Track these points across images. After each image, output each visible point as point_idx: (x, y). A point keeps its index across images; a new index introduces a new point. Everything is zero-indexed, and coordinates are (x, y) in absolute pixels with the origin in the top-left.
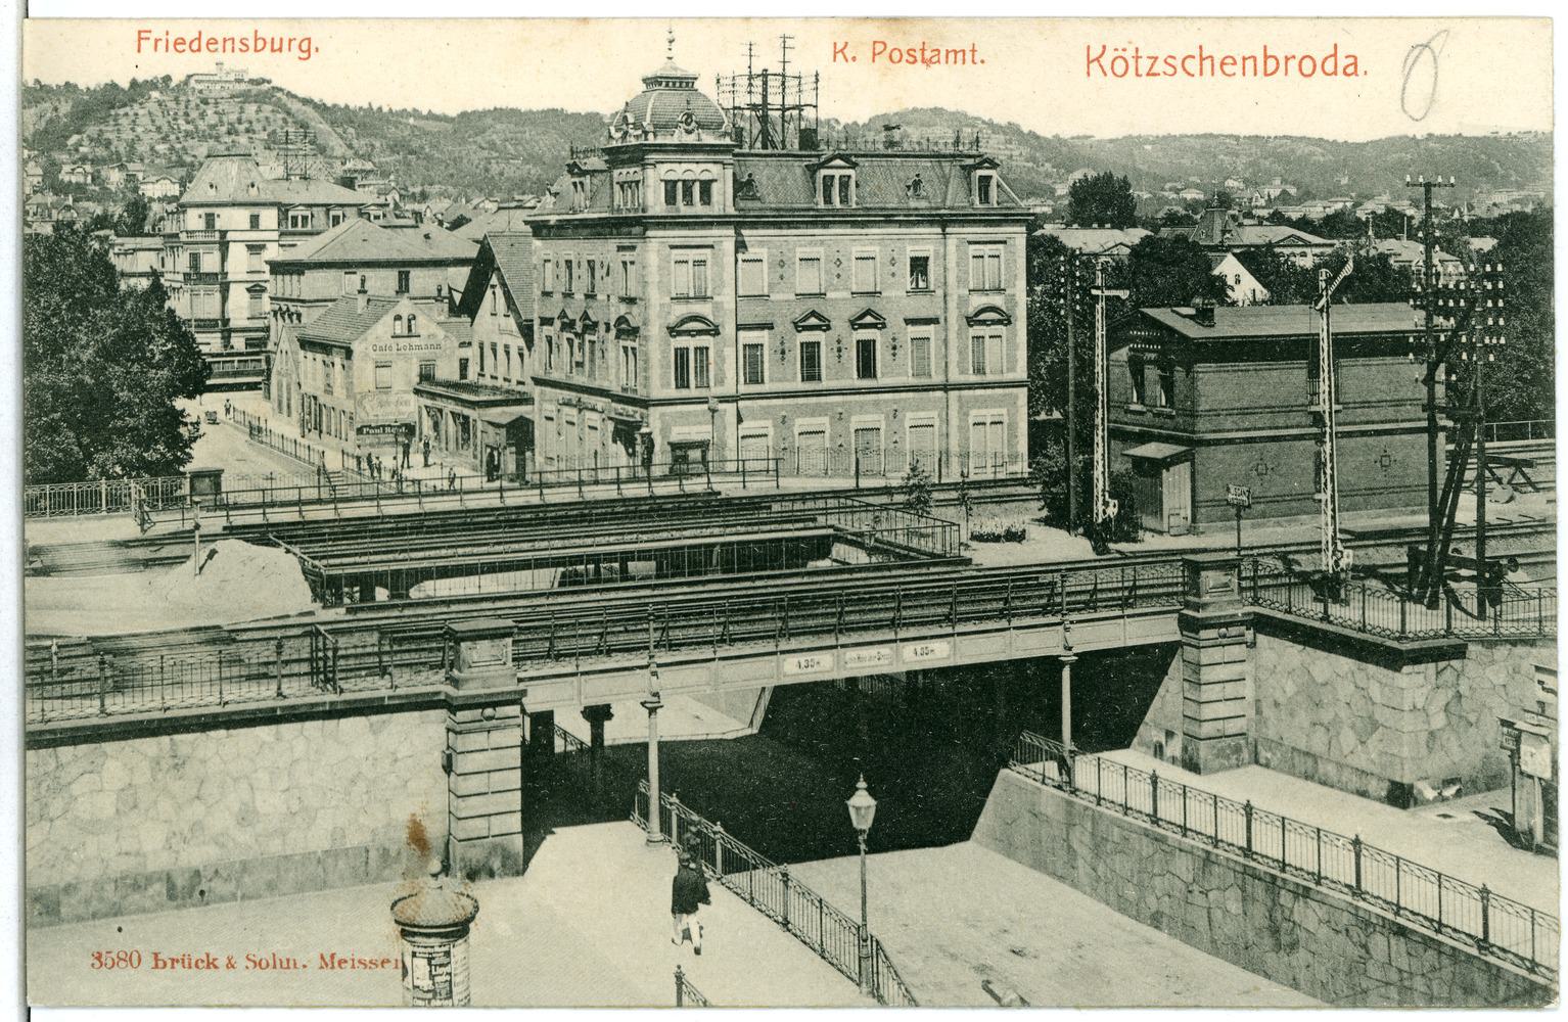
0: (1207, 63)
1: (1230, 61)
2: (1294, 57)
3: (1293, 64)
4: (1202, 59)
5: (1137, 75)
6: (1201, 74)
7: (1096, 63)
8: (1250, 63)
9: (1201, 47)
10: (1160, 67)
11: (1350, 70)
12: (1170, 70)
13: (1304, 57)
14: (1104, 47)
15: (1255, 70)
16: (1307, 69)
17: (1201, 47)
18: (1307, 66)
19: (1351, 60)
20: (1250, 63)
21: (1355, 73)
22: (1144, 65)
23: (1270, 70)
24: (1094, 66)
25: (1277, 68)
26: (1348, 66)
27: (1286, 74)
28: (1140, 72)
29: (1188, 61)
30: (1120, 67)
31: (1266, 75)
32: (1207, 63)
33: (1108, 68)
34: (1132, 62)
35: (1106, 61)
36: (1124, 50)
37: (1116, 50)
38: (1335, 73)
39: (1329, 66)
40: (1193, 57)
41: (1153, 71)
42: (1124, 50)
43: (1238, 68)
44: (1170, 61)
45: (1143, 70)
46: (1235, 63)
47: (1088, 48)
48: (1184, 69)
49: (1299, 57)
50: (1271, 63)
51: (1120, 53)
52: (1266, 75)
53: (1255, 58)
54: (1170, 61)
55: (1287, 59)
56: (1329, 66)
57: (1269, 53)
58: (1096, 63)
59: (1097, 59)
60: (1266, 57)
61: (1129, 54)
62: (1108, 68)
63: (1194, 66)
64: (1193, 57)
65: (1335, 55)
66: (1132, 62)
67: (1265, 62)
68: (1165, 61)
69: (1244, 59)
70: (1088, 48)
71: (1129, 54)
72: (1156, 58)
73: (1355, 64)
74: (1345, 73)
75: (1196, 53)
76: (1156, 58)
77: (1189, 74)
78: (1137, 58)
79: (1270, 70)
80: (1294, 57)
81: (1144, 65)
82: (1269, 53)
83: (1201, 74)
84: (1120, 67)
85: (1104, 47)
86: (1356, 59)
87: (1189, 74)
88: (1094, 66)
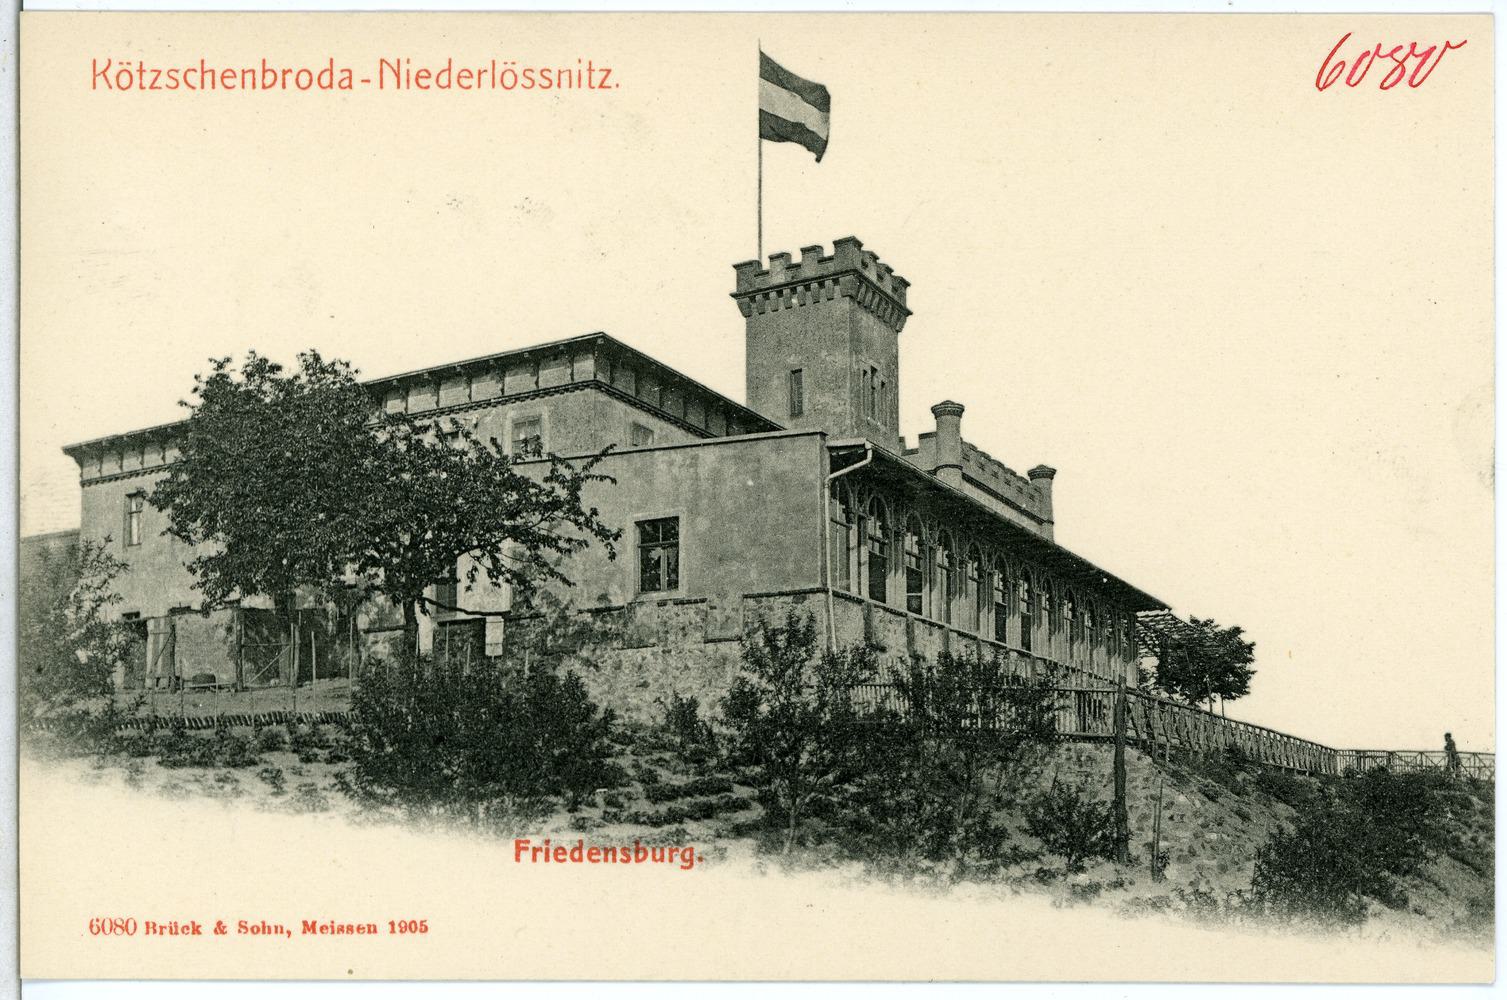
0: (208, 77)
1: (229, 74)
2: (290, 71)
3: (290, 78)
4: (203, 73)
5: (142, 87)
6: (202, 87)
8: (249, 77)
9: (203, 62)
10: (163, 80)
11: (345, 83)
12: (173, 84)
14: (110, 61)
15: (213, 83)
17: (203, 62)
18: (304, 79)
19: (347, 74)
20: (249, 77)
21: (350, 86)
22: (148, 78)
24: (100, 80)
25: (275, 80)
26: (342, 80)
27: (284, 86)
28: (144, 85)
29: (189, 75)
30: (125, 80)
31: (264, 87)
32: (208, 77)
33: (113, 81)
35: (111, 74)
36: (129, 64)
37: (121, 63)
38: (331, 86)
40: (195, 70)
42: (129, 64)
43: (237, 82)
44: (172, 74)
45: (147, 83)
49: (295, 71)
52: (264, 87)
53: (253, 72)
54: (172, 74)
55: (285, 72)
57: (267, 67)
59: (104, 72)
60: (264, 71)
61: (134, 69)
62: (113, 81)
63: (195, 79)
64: (195, 70)
67: (264, 77)
69: (244, 72)
71: (134, 69)
72: (160, 72)
73: (350, 78)
77: (189, 85)
78: (141, 71)
79: (268, 82)
80: (290, 71)
81: (148, 78)
82: (267, 67)
83: (202, 87)
84: (125, 80)
85: (110, 61)
86: (350, 71)
87: (189, 85)
88: (100, 80)
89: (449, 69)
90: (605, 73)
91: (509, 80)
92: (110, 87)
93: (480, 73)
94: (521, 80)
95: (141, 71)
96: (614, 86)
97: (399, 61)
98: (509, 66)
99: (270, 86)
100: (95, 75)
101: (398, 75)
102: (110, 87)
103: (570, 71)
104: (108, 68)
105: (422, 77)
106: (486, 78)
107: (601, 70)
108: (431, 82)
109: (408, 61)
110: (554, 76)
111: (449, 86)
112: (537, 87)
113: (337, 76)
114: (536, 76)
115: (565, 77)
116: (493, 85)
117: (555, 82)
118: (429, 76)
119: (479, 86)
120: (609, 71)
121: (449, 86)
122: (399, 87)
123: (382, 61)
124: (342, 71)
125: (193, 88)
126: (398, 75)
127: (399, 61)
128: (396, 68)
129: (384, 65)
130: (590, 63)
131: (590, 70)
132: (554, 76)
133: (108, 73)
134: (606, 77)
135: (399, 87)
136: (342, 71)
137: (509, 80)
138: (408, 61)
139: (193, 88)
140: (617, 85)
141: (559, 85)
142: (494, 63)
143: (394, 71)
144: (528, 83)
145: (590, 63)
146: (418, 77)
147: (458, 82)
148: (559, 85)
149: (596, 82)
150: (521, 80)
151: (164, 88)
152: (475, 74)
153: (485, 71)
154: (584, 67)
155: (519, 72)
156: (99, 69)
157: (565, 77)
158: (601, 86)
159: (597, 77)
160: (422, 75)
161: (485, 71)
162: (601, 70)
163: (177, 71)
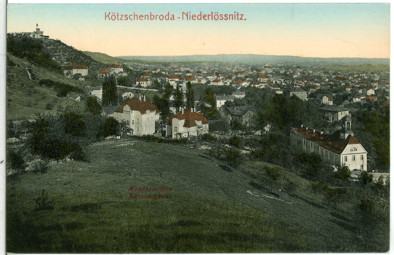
0: (136, 17)
1: (142, 16)
2: (158, 15)
3: (158, 17)
4: (134, 16)
5: (118, 20)
6: (134, 19)
7: (107, 17)
8: (147, 17)
9: (134, 13)
10: (124, 18)
11: (172, 18)
12: (126, 18)
13: (161, 15)
14: (110, 13)
16: (161, 18)
17: (134, 13)
18: (161, 17)
19: (172, 16)
20: (147, 17)
21: (173, 19)
23: (152, 18)
24: (107, 17)
26: (171, 18)
27: (156, 19)
30: (113, 18)
31: (151, 20)
32: (136, 17)
33: (110, 18)
34: (117, 16)
35: (110, 16)
36: (115, 13)
38: (168, 19)
39: (167, 17)
40: (132, 15)
41: (122, 19)
42: (115, 13)
43: (144, 18)
44: (126, 16)
46: (143, 17)
47: (106, 13)
48: (130, 18)
49: (159, 15)
51: (114, 14)
52: (151, 20)
53: (148, 16)
54: (126, 16)
56: (167, 17)
58: (107, 17)
59: (108, 16)
60: (151, 15)
61: (116, 15)
62: (110, 18)
63: (132, 17)
65: (168, 15)
66: (117, 16)
69: (145, 16)
70: (106, 13)
71: (116, 15)
73: (173, 17)
74: (171, 19)
75: (133, 15)
76: (123, 16)
78: (118, 15)
79: (152, 18)
80: (158, 15)
82: (152, 14)
83: (134, 19)
84: (113, 18)
85: (110, 13)
86: (174, 15)
88: (107, 17)
89: (201, 15)
90: (241, 16)
91: (216, 17)
92: (110, 19)
93: (209, 15)
94: (220, 17)
95: (118, 15)
96: (244, 19)
97: (187, 12)
98: (216, 14)
99: (152, 20)
100: (106, 16)
101: (187, 16)
102: (110, 19)
103: (232, 15)
104: (109, 14)
105: (193, 17)
106: (210, 17)
107: (241, 15)
108: (196, 18)
109: (190, 13)
110: (228, 17)
111: (201, 19)
112: (224, 19)
113: (170, 16)
114: (224, 17)
115: (231, 16)
116: (212, 19)
117: (229, 19)
118: (195, 17)
119: (208, 19)
120: (242, 15)
121: (201, 19)
122: (187, 19)
123: (183, 13)
124: (172, 15)
125: (132, 20)
126: (187, 16)
127: (187, 12)
128: (187, 14)
129: (184, 13)
130: (238, 13)
131: (238, 15)
132: (228, 16)
133: (109, 16)
134: (242, 17)
135: (187, 19)
136: (172, 15)
137: (216, 17)
138: (190, 13)
139: (132, 20)
140: (245, 20)
141: (230, 19)
142: (212, 13)
143: (186, 15)
144: (221, 18)
145: (238, 13)
146: (192, 17)
147: (204, 17)
148: (230, 19)
149: (239, 18)
150: (220, 17)
151: (124, 20)
152: (207, 16)
153: (210, 15)
154: (236, 14)
155: (219, 15)
156: (107, 14)
157: (231, 16)
158: (241, 19)
159: (240, 17)
160: (194, 16)
161: (210, 15)
162: (241, 15)
163: (127, 15)
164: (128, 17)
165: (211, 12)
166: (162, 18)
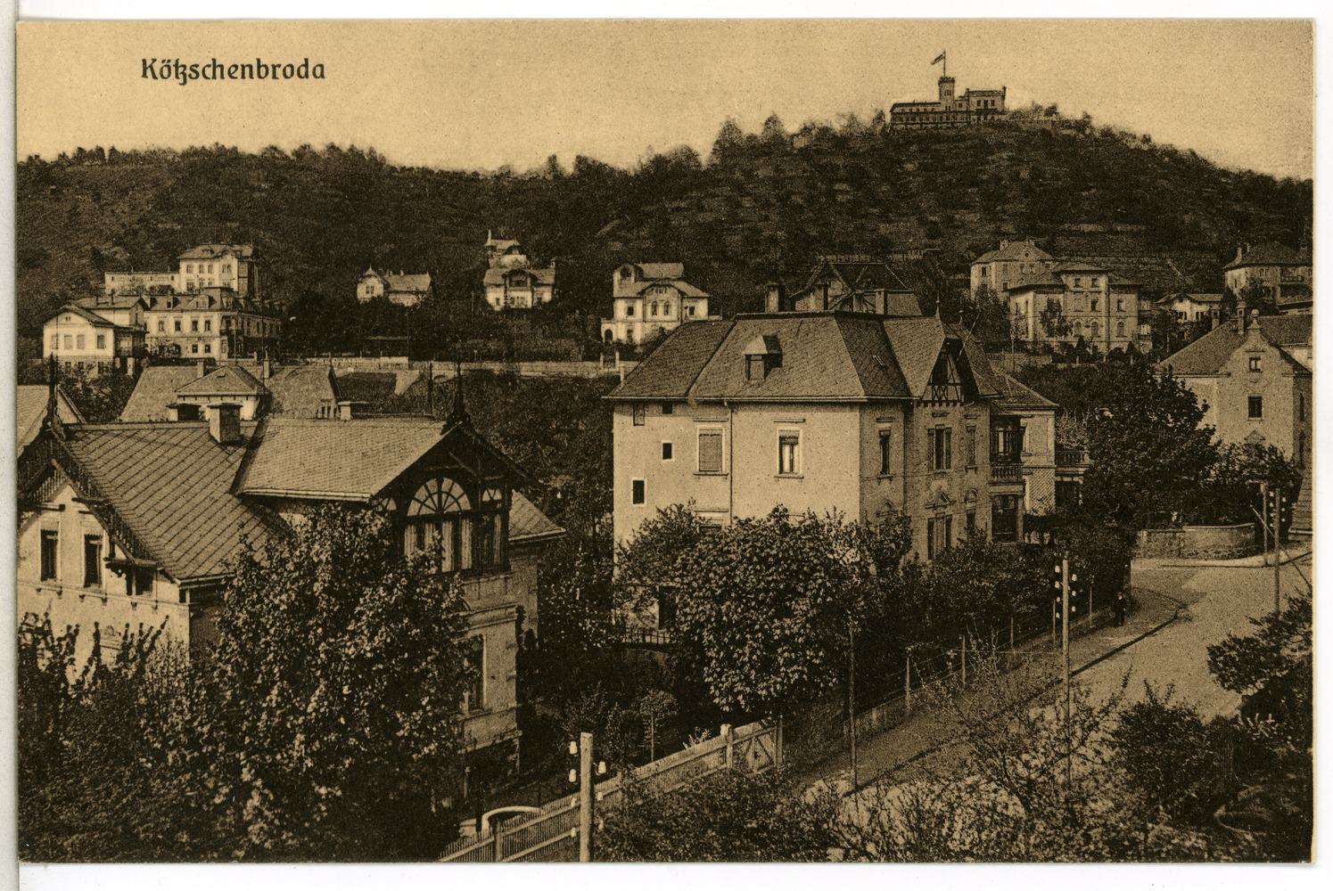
0: (218, 70)
2: (279, 66)
3: (279, 72)
8: (247, 70)
12: (194, 75)
23: (263, 74)
30: (165, 73)
32: (218, 70)
40: (209, 66)
42: (169, 61)
49: (282, 67)
50: (263, 70)
53: (251, 67)
55: (274, 67)
60: (259, 67)
61: (171, 64)
62: (157, 73)
63: (209, 72)
66: (173, 69)
68: (191, 69)
71: (171, 64)
75: (211, 63)
88: (149, 72)
164: (199, 70)
165: (1054, 101)
166: (291, 71)
